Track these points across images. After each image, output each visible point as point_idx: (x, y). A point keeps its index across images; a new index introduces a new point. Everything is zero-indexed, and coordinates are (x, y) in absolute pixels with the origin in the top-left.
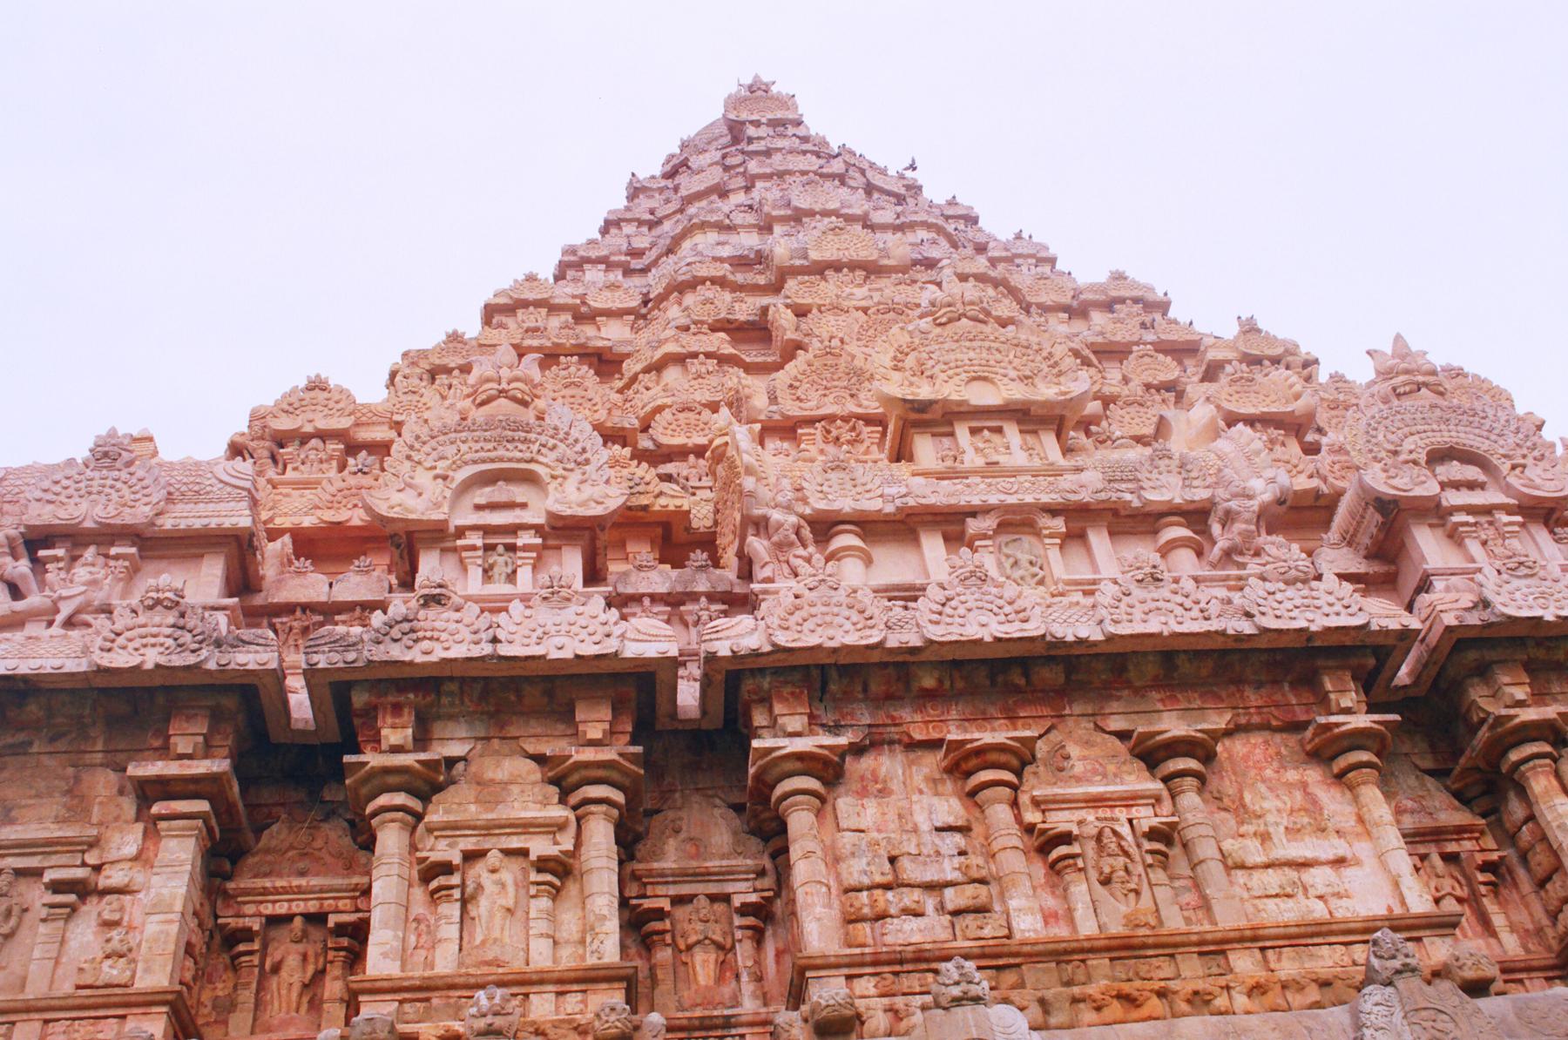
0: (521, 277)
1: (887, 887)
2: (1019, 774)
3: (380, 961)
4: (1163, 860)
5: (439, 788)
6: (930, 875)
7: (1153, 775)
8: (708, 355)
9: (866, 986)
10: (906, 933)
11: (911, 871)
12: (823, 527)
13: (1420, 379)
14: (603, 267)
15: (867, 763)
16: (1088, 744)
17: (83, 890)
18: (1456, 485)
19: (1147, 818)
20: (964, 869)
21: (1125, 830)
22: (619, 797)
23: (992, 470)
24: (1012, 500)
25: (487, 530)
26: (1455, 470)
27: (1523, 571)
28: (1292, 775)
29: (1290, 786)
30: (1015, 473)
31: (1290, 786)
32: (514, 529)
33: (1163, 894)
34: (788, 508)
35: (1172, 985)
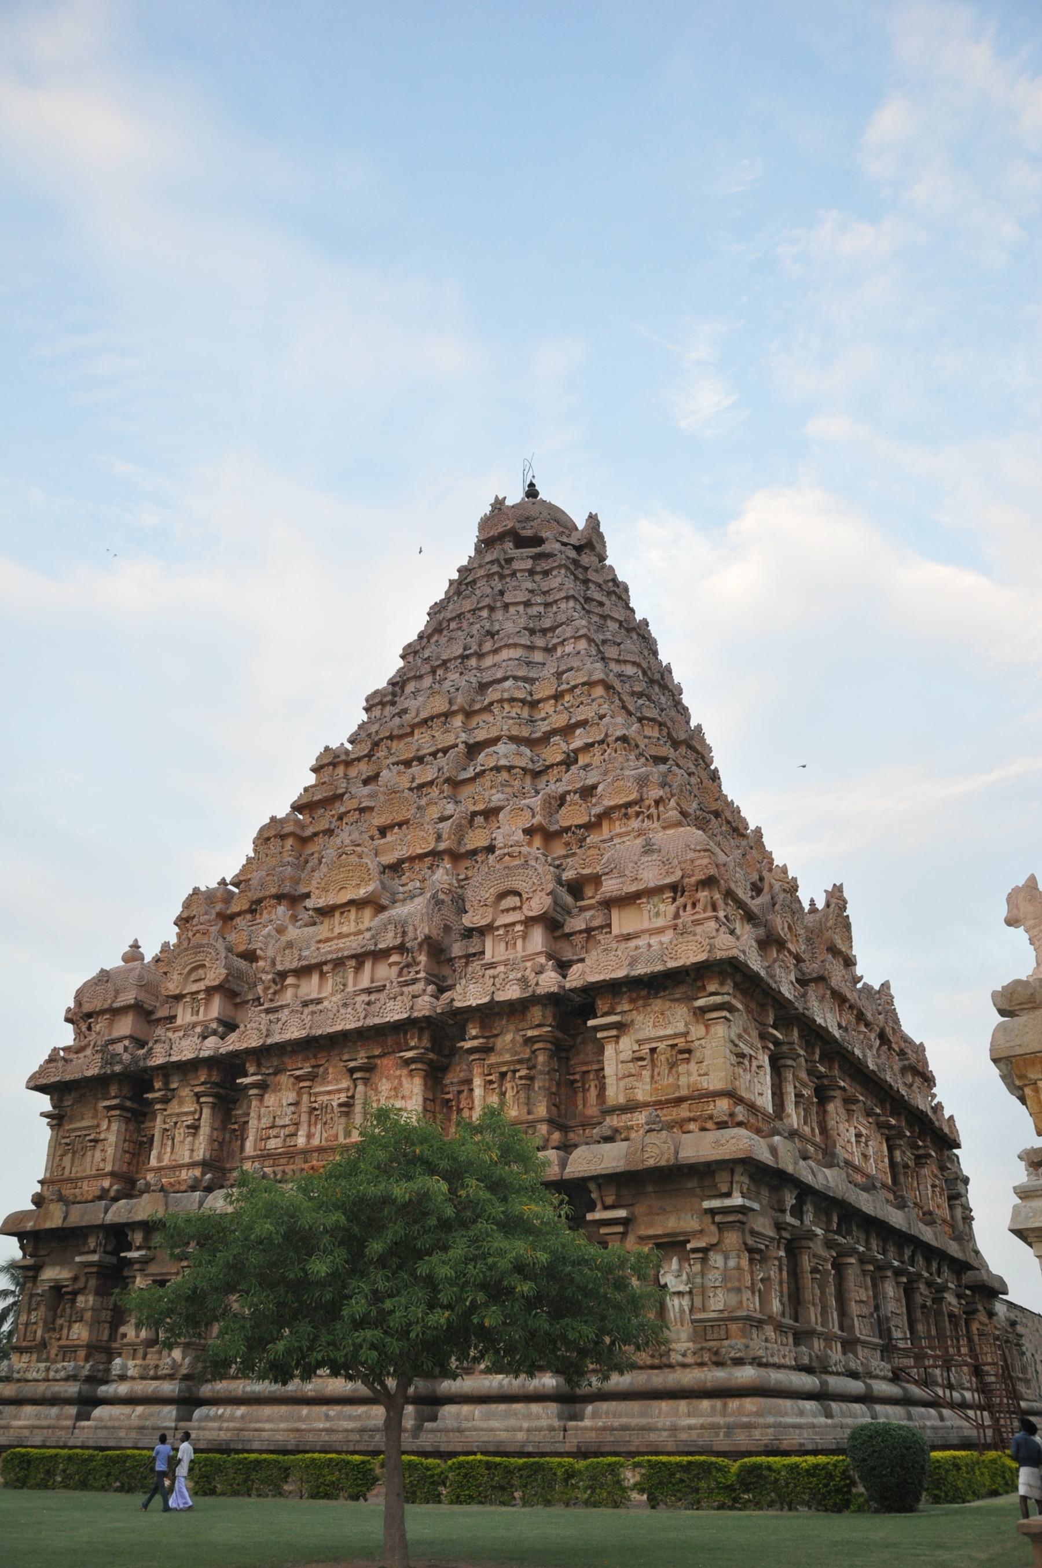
0: (322, 750)
1: (270, 1128)
2: (312, 1080)
3: (153, 1162)
5: (170, 1100)
7: (351, 1076)
8: (355, 810)
10: (272, 1144)
11: (279, 1122)
12: (282, 975)
13: (506, 851)
14: (379, 707)
15: (278, 1077)
16: (335, 1067)
18: (507, 910)
19: (343, 1097)
20: (291, 1120)
21: (335, 1104)
22: (210, 1099)
23: (341, 936)
24: (335, 956)
25: (192, 993)
27: (474, 981)
28: (398, 1072)
29: (396, 1077)
30: (348, 935)
31: (396, 1077)
32: (198, 992)
33: (341, 1128)
34: (267, 973)
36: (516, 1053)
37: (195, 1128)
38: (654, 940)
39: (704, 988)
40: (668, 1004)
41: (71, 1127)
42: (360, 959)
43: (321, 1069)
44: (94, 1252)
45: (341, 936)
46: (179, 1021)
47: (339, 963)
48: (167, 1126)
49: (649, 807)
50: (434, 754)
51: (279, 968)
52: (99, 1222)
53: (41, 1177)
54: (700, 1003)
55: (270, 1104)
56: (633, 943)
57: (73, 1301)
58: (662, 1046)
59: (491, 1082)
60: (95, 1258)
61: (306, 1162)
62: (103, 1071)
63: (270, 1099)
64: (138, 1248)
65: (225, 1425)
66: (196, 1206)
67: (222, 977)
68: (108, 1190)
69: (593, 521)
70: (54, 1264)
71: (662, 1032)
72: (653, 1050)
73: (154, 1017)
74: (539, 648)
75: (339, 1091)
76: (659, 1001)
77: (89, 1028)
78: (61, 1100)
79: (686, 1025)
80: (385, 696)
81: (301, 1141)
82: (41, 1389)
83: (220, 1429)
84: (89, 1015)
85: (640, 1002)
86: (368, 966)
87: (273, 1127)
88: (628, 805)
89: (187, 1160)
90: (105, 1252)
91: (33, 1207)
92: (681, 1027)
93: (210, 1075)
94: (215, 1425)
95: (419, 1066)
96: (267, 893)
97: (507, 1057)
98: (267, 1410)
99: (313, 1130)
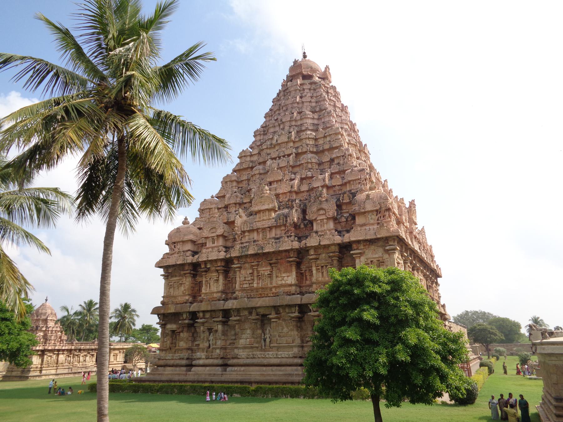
3: (203, 291)
4: (270, 277)
6: (248, 279)
9: (240, 292)
10: (245, 286)
11: (246, 279)
12: (244, 232)
15: (245, 265)
17: (181, 284)
22: (222, 271)
23: (263, 220)
26: (322, 212)
28: (287, 264)
33: (269, 281)
34: (239, 231)
35: (265, 293)
36: (326, 260)
37: (217, 281)
38: (371, 227)
39: (388, 243)
40: (376, 247)
41: (172, 279)
42: (270, 228)
43: (260, 263)
44: (185, 319)
45: (263, 220)
46: (207, 246)
47: (264, 229)
48: (208, 280)
49: (363, 181)
50: (284, 156)
51: (242, 230)
52: (188, 311)
53: (163, 295)
54: (387, 248)
55: (243, 273)
56: (364, 228)
57: (179, 335)
58: (375, 260)
59: (319, 269)
60: (187, 321)
61: (257, 292)
62: (183, 262)
63: (243, 272)
64: (201, 319)
65: (239, 373)
66: (222, 306)
67: (222, 232)
68: (188, 300)
69: (327, 68)
70: (171, 323)
71: (374, 256)
72: (372, 261)
73: (196, 243)
74: (315, 119)
75: (267, 270)
76: (373, 246)
77: (175, 247)
78: (167, 270)
79: (382, 254)
80: (261, 132)
81: (255, 285)
82: (172, 362)
83: (237, 374)
84: (174, 243)
85: (367, 246)
86: (274, 230)
87: (245, 280)
88: (355, 180)
89: (215, 291)
90: (189, 320)
91: (161, 305)
92: (380, 254)
93: (221, 264)
94: (235, 373)
95: (294, 263)
96: (231, 202)
97: (323, 261)
98: (252, 368)
99: (259, 282)
